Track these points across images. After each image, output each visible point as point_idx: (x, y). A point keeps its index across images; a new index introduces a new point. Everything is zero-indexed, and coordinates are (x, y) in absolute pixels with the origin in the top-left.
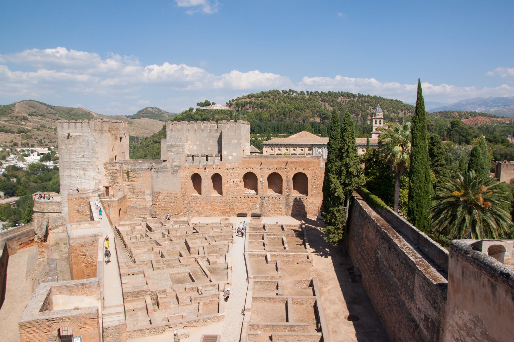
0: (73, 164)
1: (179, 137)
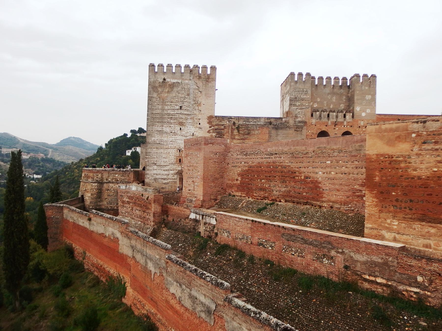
0: (166, 116)
1: (305, 90)
